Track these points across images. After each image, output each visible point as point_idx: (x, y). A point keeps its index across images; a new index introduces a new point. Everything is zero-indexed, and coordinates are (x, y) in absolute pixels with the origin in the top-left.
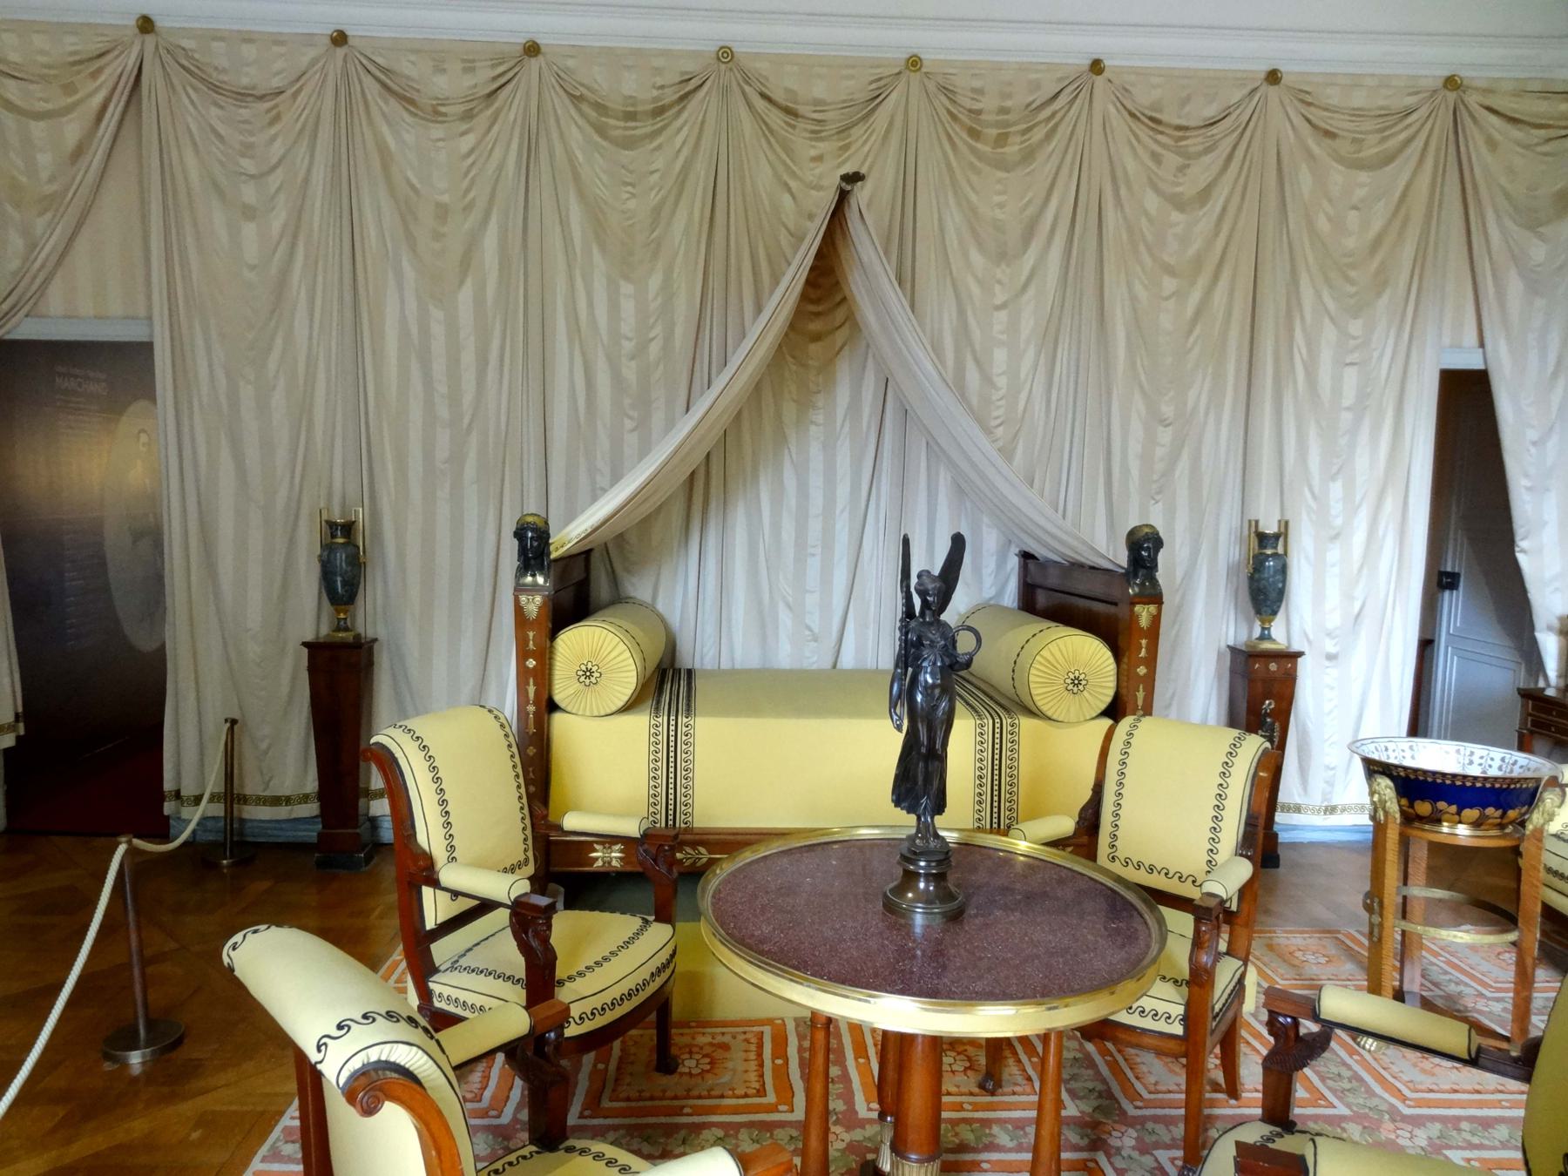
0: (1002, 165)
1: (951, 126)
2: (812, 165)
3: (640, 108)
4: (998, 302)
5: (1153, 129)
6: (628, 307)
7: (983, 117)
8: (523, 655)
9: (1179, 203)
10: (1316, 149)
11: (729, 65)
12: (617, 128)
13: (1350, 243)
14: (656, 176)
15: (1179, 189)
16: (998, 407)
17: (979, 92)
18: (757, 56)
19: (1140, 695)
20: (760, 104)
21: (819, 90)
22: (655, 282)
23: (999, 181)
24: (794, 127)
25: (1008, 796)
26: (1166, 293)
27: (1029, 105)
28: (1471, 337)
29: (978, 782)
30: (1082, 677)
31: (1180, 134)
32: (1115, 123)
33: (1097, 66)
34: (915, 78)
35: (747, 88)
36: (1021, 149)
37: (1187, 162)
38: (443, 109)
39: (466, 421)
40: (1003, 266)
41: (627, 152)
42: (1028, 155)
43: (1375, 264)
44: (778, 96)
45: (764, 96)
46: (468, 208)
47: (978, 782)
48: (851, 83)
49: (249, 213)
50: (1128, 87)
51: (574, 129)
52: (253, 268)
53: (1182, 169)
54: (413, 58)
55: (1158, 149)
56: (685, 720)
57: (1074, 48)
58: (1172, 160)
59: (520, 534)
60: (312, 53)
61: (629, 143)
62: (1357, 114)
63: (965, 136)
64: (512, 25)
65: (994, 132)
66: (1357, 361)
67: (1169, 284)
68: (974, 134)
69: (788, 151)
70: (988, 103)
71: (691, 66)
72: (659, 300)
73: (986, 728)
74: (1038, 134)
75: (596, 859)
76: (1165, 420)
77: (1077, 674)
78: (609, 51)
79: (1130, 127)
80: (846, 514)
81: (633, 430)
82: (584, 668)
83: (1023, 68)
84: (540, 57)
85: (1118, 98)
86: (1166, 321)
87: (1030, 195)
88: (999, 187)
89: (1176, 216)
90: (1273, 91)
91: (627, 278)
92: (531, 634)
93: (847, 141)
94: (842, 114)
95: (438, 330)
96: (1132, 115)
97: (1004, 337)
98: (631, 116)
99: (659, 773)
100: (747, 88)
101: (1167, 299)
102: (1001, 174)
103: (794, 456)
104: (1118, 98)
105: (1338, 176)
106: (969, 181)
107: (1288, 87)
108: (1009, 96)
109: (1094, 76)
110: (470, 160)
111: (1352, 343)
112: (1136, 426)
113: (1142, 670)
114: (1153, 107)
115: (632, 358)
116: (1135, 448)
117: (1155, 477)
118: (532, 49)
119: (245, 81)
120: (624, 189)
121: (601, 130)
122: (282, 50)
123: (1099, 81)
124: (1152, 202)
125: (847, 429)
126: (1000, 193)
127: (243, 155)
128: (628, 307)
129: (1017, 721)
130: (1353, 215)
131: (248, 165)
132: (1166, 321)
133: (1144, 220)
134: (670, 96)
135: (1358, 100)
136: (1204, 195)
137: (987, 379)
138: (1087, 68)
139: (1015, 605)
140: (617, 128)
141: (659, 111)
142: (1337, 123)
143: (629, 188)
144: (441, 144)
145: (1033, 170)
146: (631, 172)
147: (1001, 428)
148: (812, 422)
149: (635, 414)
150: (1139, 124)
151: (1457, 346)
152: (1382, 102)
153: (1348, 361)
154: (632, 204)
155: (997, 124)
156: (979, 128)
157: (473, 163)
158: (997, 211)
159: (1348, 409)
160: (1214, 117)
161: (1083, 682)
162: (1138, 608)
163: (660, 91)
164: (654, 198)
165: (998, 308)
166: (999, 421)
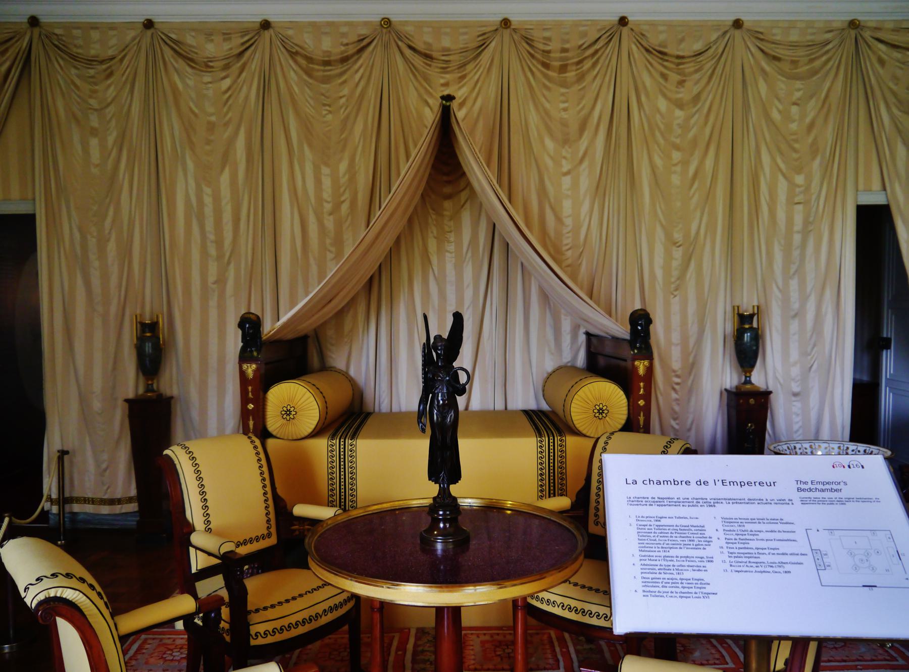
0: (564, 84)
1: (531, 62)
2: (442, 89)
3: (332, 58)
4: (565, 170)
5: (661, 59)
6: (327, 182)
7: (552, 55)
8: (245, 400)
9: (680, 105)
10: (767, 68)
11: (389, 29)
12: (318, 70)
13: (794, 126)
14: (343, 100)
15: (680, 96)
16: (568, 238)
17: (549, 39)
18: (406, 23)
19: (642, 418)
20: (408, 52)
21: (446, 42)
22: (343, 167)
23: (563, 94)
24: (430, 66)
25: (560, 486)
26: (675, 162)
27: (580, 47)
28: (876, 185)
29: (540, 478)
30: (604, 408)
31: (680, 61)
32: (636, 56)
33: (623, 21)
34: (507, 33)
35: (400, 43)
36: (577, 75)
37: (684, 78)
38: (211, 64)
39: (228, 255)
41: (324, 86)
42: (581, 78)
43: (810, 140)
44: (420, 46)
45: (410, 47)
46: (226, 124)
47: (540, 478)
48: (466, 37)
49: (94, 132)
50: (644, 33)
51: (292, 73)
52: (97, 166)
53: (681, 83)
54: (193, 34)
55: (666, 71)
56: (350, 441)
57: (610, 12)
58: (674, 77)
59: (241, 325)
60: (132, 34)
61: (326, 80)
62: (794, 46)
63: (540, 67)
64: (253, 13)
65: (557, 64)
66: (802, 201)
67: (676, 156)
68: (546, 66)
69: (426, 79)
70: (554, 46)
71: (364, 31)
72: (347, 177)
73: (544, 443)
74: (587, 64)
75: (295, 530)
76: (677, 243)
77: (601, 406)
78: (313, 25)
79: (648, 61)
80: (471, 309)
81: (332, 260)
82: (285, 409)
83: (577, 24)
84: (271, 31)
85: (637, 40)
86: (676, 180)
87: (584, 102)
88: (562, 98)
89: (678, 113)
90: (737, 33)
91: (326, 164)
92: (250, 388)
93: (464, 73)
94: (461, 56)
95: (208, 200)
96: (647, 50)
97: (569, 193)
98: (327, 63)
99: (335, 475)
100: (400, 43)
101: (675, 165)
102: (563, 90)
103: (436, 273)
104: (637, 40)
105: (782, 85)
106: (544, 96)
107: (748, 30)
108: (568, 42)
109: (621, 27)
110: (227, 95)
111: (798, 190)
112: (659, 249)
113: (641, 403)
114: (660, 46)
115: (331, 214)
116: (659, 261)
117: (673, 280)
118: (266, 25)
119: (93, 52)
120: (324, 108)
121: (309, 73)
122: (114, 32)
123: (625, 30)
124: (662, 104)
125: (469, 254)
127: (91, 97)
128: (327, 182)
129: (564, 438)
130: (794, 109)
131: (93, 102)
132: (676, 180)
133: (658, 116)
134: (352, 50)
135: (794, 37)
136: (696, 98)
137: (559, 219)
138: (617, 23)
139: (585, 366)
140: (318, 70)
141: (344, 60)
142: (780, 52)
143: (327, 108)
144: (210, 85)
145: (584, 87)
146: (327, 97)
148: (448, 251)
149: (333, 249)
150: (651, 55)
151: (868, 190)
152: (809, 38)
153: (796, 201)
154: (330, 117)
155: (561, 59)
156: (548, 62)
157: (230, 96)
158: (563, 113)
159: (798, 232)
160: (701, 50)
161: (606, 412)
162: (637, 363)
163: (347, 47)
164: (342, 114)
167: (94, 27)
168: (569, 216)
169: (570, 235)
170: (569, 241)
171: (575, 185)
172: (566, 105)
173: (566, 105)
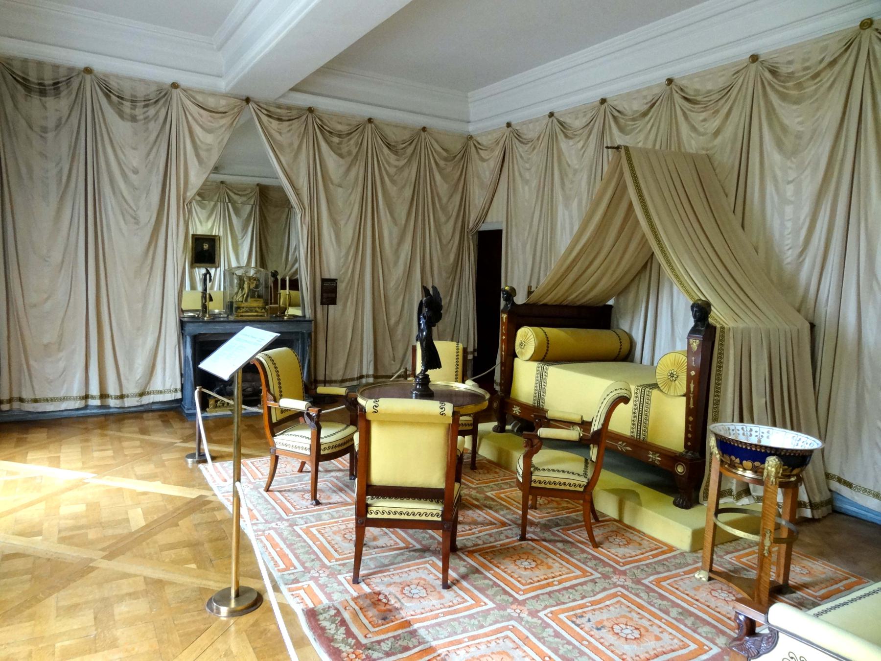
2: (703, 123)
4: (790, 179)
7: (796, 75)
16: (789, 239)
21: (709, 86)
40: (793, 159)
48: (723, 78)
60: (545, 122)
97: (793, 199)
102: (795, 107)
108: (807, 60)
126: (798, 117)
147: (790, 251)
165: (789, 183)
166: (788, 247)
167: (531, 121)
168: (789, 220)
169: (790, 236)
170: (789, 242)
171: (798, 192)
172: (800, 119)
173: (800, 119)
